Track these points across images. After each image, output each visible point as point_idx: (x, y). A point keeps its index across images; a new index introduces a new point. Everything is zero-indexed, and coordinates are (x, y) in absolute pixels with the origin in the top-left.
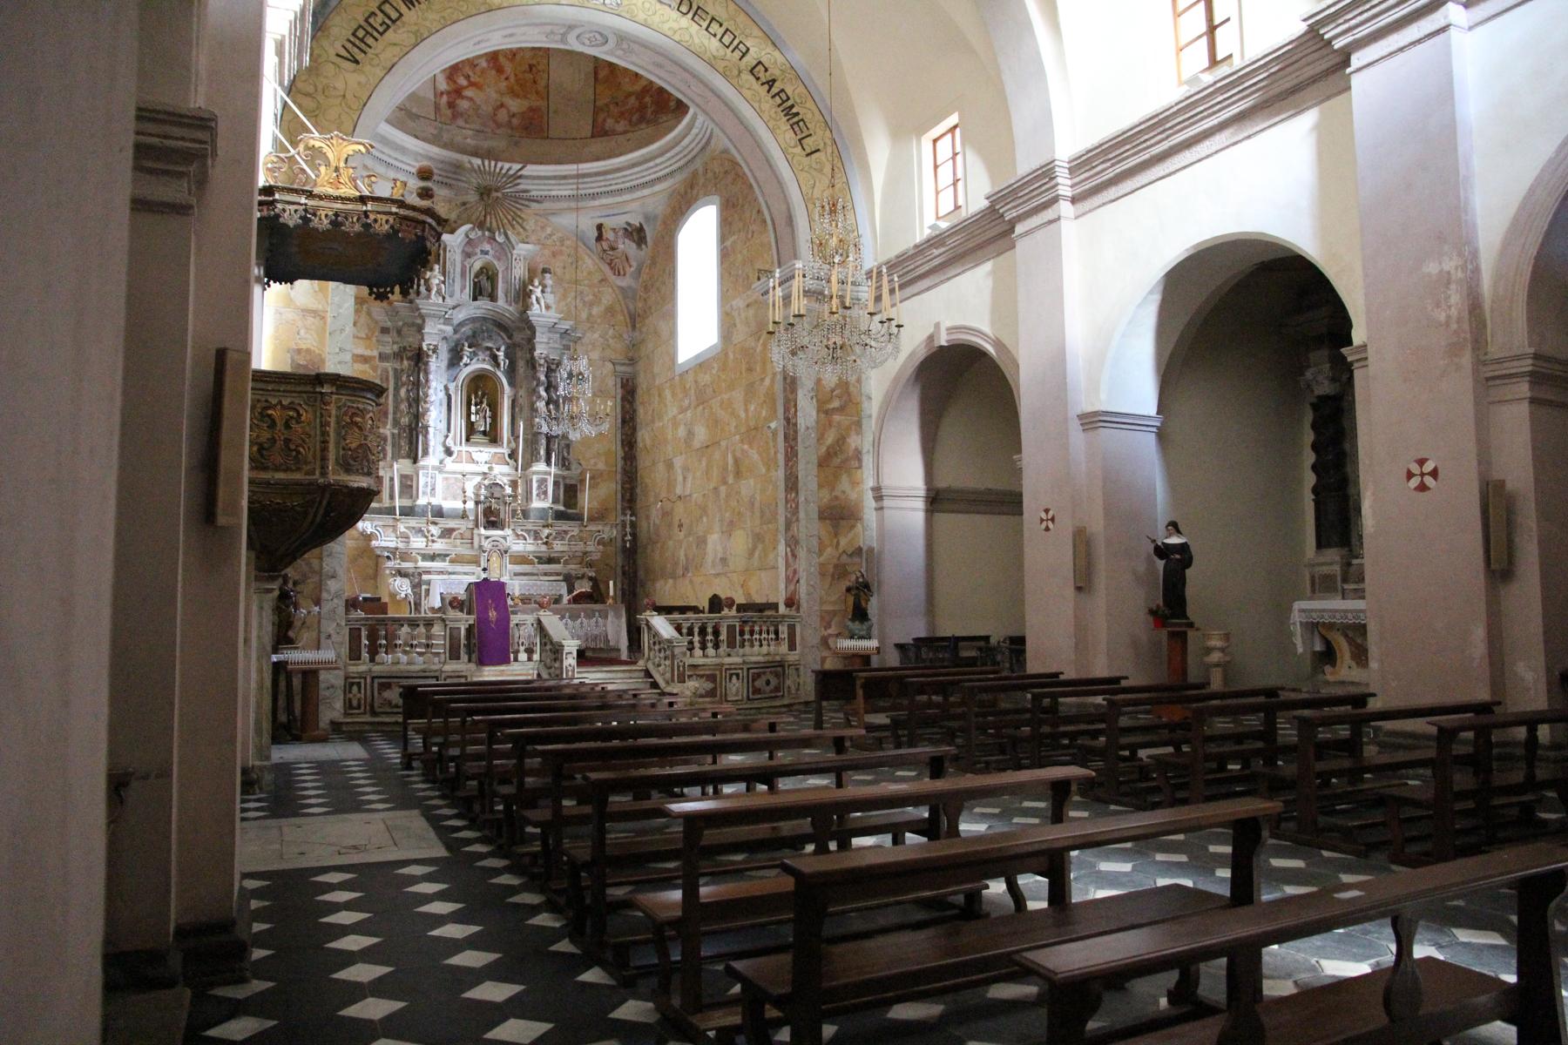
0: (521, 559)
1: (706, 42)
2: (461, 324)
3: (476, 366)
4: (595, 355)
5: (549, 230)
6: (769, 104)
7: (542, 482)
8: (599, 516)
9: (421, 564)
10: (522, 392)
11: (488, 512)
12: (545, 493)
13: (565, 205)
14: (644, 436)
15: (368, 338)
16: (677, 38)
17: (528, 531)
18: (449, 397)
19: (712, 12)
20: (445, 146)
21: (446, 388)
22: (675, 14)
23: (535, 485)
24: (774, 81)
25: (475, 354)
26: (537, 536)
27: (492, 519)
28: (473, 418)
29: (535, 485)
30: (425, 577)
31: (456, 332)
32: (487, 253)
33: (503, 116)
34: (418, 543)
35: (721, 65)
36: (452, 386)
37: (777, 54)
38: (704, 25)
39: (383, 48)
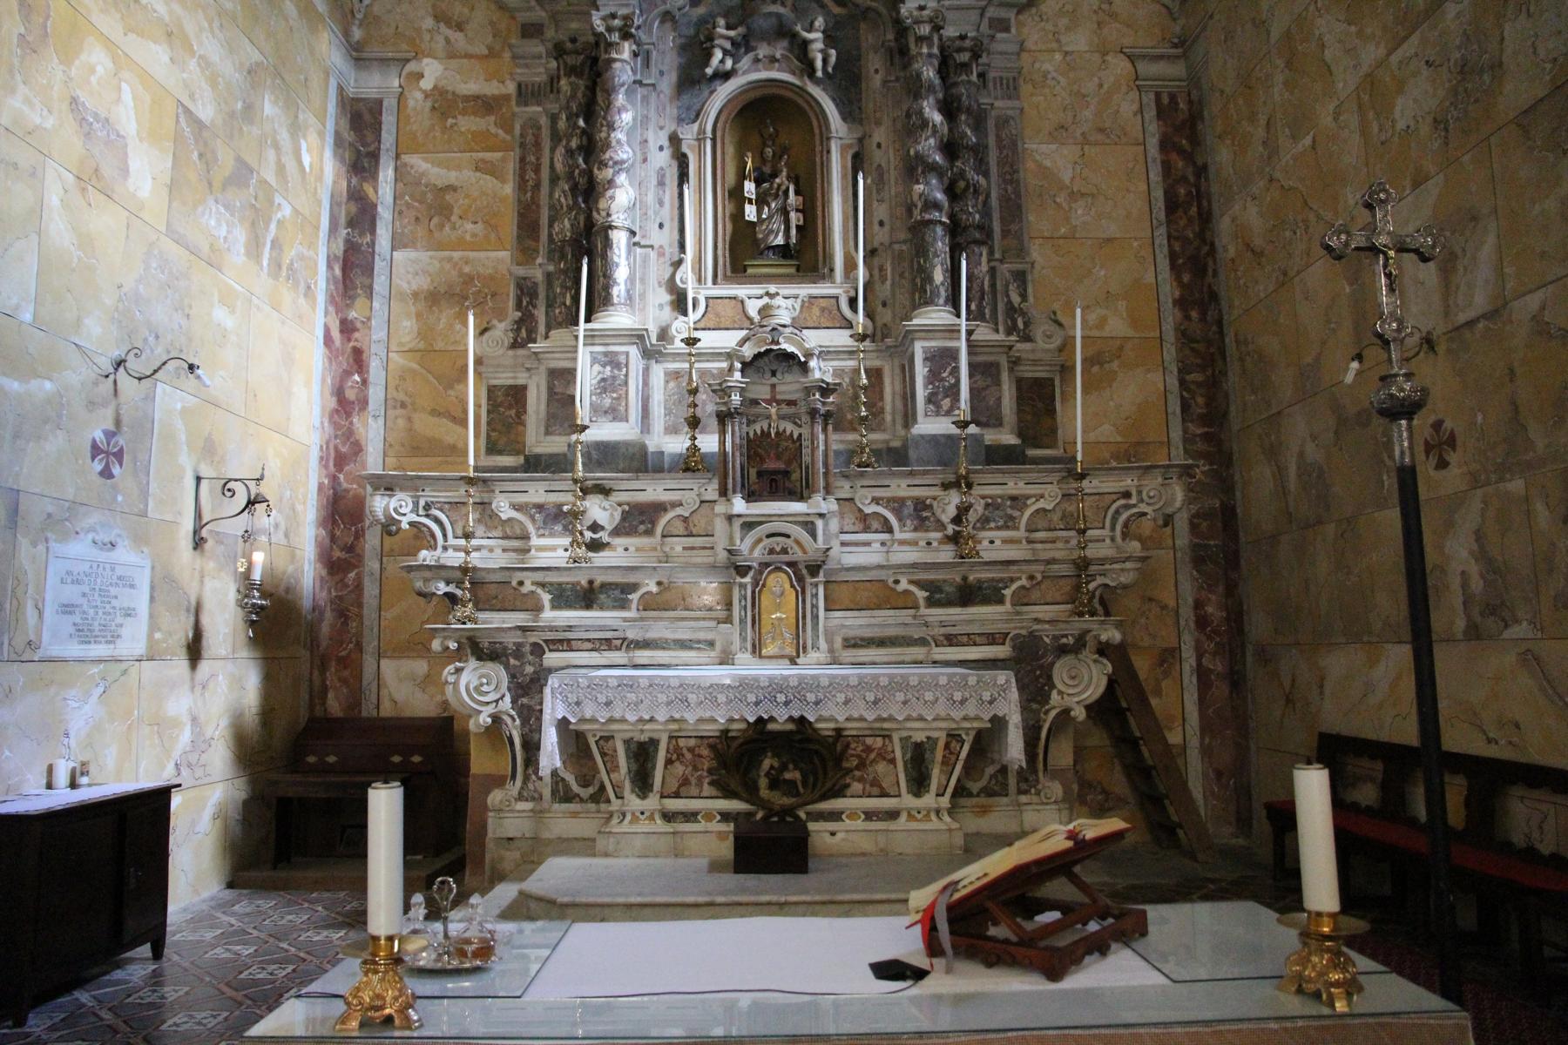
3: (749, 74)
4: (1079, 41)
7: (942, 360)
8: (1131, 454)
9: (552, 616)
10: (880, 135)
11: (755, 448)
12: (953, 392)
14: (1241, 218)
15: (492, 54)
17: (897, 505)
18: (682, 161)
21: (675, 140)
23: (921, 371)
25: (740, 47)
26: (921, 514)
27: (771, 469)
28: (750, 212)
29: (921, 371)
30: (551, 658)
34: (552, 551)
36: (688, 134)
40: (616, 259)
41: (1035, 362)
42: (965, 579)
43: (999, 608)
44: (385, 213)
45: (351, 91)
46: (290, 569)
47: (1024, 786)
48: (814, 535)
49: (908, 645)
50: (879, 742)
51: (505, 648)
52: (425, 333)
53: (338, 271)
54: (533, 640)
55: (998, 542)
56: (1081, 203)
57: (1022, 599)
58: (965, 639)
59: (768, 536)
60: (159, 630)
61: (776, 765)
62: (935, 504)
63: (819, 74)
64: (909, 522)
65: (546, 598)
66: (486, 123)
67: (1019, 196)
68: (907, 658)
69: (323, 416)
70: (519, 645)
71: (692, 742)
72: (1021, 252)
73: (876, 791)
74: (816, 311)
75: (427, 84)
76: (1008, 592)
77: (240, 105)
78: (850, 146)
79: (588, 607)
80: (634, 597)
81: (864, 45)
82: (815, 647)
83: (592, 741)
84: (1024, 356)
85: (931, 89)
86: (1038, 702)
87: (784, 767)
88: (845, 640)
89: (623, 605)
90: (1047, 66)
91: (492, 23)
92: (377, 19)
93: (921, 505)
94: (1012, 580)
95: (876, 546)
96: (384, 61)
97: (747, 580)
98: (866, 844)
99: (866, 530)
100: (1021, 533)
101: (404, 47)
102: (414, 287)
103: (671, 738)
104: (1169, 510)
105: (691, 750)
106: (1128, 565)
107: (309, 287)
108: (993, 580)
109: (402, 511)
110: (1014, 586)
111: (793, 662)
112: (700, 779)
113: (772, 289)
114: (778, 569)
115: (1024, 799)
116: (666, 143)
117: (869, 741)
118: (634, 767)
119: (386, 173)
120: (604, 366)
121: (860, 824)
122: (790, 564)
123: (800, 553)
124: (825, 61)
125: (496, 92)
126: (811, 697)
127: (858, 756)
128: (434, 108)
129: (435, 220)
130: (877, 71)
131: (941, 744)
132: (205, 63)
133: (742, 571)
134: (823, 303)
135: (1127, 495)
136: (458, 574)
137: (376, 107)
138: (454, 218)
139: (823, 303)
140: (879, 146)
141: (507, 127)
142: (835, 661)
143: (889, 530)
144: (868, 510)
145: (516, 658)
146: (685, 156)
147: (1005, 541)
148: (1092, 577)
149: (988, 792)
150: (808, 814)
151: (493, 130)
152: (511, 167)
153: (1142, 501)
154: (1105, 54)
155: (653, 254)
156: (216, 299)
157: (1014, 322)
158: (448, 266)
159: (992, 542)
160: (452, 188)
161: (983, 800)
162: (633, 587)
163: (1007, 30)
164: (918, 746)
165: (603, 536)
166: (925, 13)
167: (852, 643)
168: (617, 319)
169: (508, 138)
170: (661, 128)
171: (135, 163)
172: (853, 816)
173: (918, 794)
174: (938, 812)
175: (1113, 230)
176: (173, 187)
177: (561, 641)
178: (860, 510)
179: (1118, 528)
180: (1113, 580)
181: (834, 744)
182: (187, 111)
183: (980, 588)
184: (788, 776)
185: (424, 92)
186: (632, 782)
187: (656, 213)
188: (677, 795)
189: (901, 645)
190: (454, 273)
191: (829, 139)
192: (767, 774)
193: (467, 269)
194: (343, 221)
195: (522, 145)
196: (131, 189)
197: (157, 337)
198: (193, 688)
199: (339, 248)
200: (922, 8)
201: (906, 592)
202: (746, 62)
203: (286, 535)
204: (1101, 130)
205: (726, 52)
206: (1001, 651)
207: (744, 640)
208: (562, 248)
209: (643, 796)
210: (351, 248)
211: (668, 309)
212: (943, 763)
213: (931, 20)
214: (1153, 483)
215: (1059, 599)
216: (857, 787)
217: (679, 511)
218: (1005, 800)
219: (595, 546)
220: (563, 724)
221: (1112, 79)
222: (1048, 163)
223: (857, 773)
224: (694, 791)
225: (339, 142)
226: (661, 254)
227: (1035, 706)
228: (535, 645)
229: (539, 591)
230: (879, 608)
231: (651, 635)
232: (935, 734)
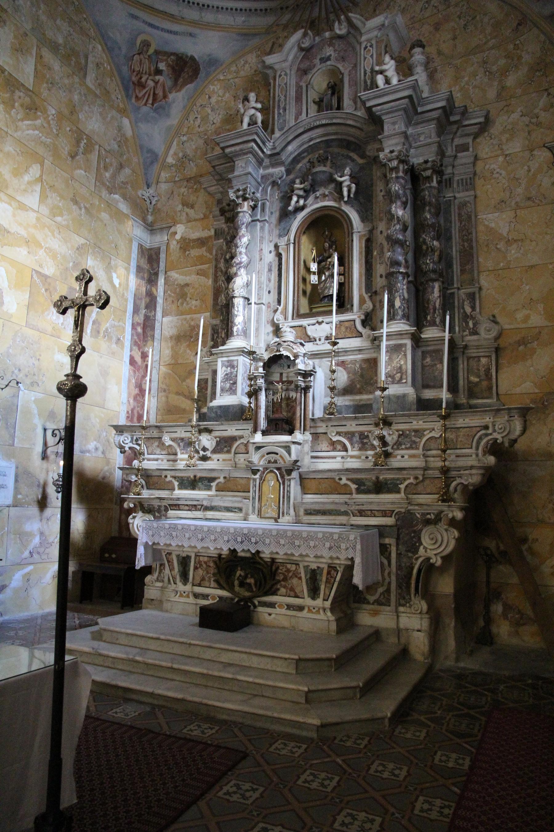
0: (330, 483)
2: (296, 160)
3: (313, 205)
15: (206, 217)
17: (350, 435)
18: (279, 256)
21: (276, 247)
25: (307, 192)
26: (363, 441)
31: (288, 172)
32: (329, 59)
36: (282, 243)
40: (236, 313)
41: (478, 347)
42: (377, 478)
43: (397, 496)
44: (160, 300)
45: (148, 245)
46: (106, 468)
47: (402, 602)
48: (290, 454)
49: (339, 515)
50: (293, 567)
51: (154, 508)
52: (175, 355)
53: (139, 330)
54: (164, 504)
55: (406, 457)
56: (515, 246)
57: (411, 490)
58: (369, 513)
59: (268, 454)
60: (21, 494)
61: (243, 574)
62: (370, 435)
63: (346, 199)
64: (356, 445)
65: (176, 484)
66: (202, 251)
67: (471, 248)
68: (337, 522)
69: (129, 397)
70: (160, 506)
71: (206, 559)
72: (472, 281)
73: (292, 594)
74: (343, 329)
75: (178, 237)
76: (402, 487)
77: (71, 264)
78: (365, 235)
79: (193, 489)
80: (214, 484)
81: (375, 178)
82: (288, 514)
83: (164, 554)
84: (471, 344)
85: (398, 196)
86: (413, 553)
87: (246, 577)
88: (305, 510)
89: (209, 488)
90: (492, 166)
91: (206, 202)
92: (159, 210)
93: (363, 436)
94: (405, 479)
95: (339, 459)
96: (162, 229)
97: (257, 476)
98: (286, 624)
99: (334, 450)
100: (420, 451)
101: (170, 221)
102: (171, 334)
103: (196, 556)
104: (513, 437)
105: (205, 563)
106: (474, 471)
107: (119, 339)
108: (393, 479)
109: (126, 442)
110: (406, 483)
111: (276, 520)
112: (209, 578)
113: (320, 319)
114: (272, 471)
115: (401, 609)
116: (272, 248)
117: (289, 566)
118: (181, 569)
119: (161, 281)
120: (227, 368)
121: (284, 611)
122: (278, 469)
123: (282, 463)
124: (349, 191)
125: (206, 235)
126: (253, 540)
127: (283, 574)
128: (181, 248)
129: (180, 301)
130: (381, 191)
131: (325, 572)
132: (49, 250)
133: (255, 472)
134: (347, 324)
135: (486, 427)
136: (136, 471)
137: (157, 251)
138: (188, 299)
139: (347, 324)
140: (381, 232)
141: (210, 251)
142: (298, 521)
143: (346, 450)
144: (334, 439)
145: (158, 512)
146: (281, 254)
147: (411, 456)
148: (454, 478)
149: (378, 602)
150: (259, 602)
151: (205, 254)
152: (211, 271)
153: (494, 431)
154: (532, 150)
155: (264, 307)
156: (56, 350)
157: (467, 323)
158: (184, 323)
159: (403, 457)
160: (187, 285)
161: (375, 607)
162: (212, 479)
163: (467, 150)
164: (313, 572)
165: (208, 454)
166: (393, 154)
167: (308, 513)
168: (235, 343)
169: (211, 257)
170: (271, 242)
171: (6, 299)
172: (281, 606)
173: (313, 598)
174: (324, 610)
175: (534, 260)
176: (30, 306)
177: (175, 505)
178: (331, 439)
179: (480, 448)
180: (467, 480)
181: (272, 565)
182: (37, 272)
183: (386, 484)
184: (248, 581)
185: (177, 240)
186: (180, 576)
187: (267, 286)
188: (199, 585)
189: (335, 515)
190: (187, 325)
191: (352, 233)
192: (238, 579)
193: (192, 323)
194: (143, 305)
195: (216, 260)
196: (5, 310)
197: (20, 370)
198: (41, 520)
199: (140, 319)
200: (392, 152)
201: (345, 485)
202: (311, 199)
203: (103, 453)
204: (529, 199)
205: (299, 197)
206: (389, 521)
207: (254, 508)
208: (222, 309)
209: (185, 584)
210: (147, 318)
211: (271, 335)
212: (326, 582)
213: (397, 158)
214: (502, 420)
215: (434, 491)
216: (283, 590)
217: (242, 441)
218: (388, 608)
219: (204, 459)
220: (146, 545)
221: (537, 165)
222: (493, 225)
223: (283, 583)
224: (207, 584)
225: (139, 269)
226: (269, 307)
227: (410, 555)
228: (165, 506)
229: (173, 480)
230: (331, 493)
231: (214, 504)
232: (321, 566)
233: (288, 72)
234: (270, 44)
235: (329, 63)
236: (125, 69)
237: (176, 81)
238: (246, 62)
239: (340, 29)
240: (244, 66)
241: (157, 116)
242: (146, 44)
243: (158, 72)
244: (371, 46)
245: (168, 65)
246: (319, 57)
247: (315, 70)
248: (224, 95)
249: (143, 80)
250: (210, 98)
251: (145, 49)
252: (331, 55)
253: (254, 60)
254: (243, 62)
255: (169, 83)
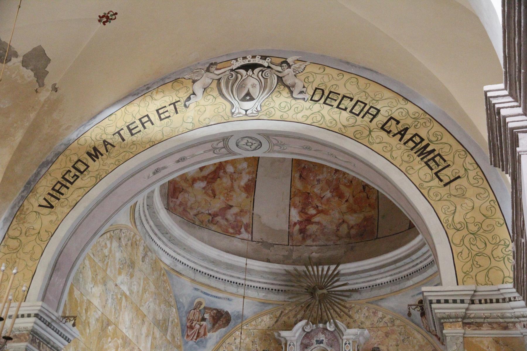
1: (336, 117)
5: (380, 314)
6: (400, 150)
13: (388, 290)
16: (309, 121)
19: (342, 91)
20: (294, 263)
22: (309, 104)
24: (406, 129)
33: (344, 229)
35: (350, 132)
37: (409, 107)
38: (336, 104)
39: (71, 194)
233: (295, 343)
234: (279, 312)
235: (321, 345)
236: (184, 319)
237: (214, 325)
238: (262, 320)
239: (330, 327)
240: (261, 322)
241: (198, 347)
242: (200, 304)
243: (204, 319)
244: (349, 344)
245: (211, 316)
246: (315, 339)
247: (313, 347)
248: (245, 339)
249: (193, 324)
250: (235, 339)
251: (198, 306)
252: (323, 340)
253: (268, 320)
254: (260, 320)
255: (209, 326)
